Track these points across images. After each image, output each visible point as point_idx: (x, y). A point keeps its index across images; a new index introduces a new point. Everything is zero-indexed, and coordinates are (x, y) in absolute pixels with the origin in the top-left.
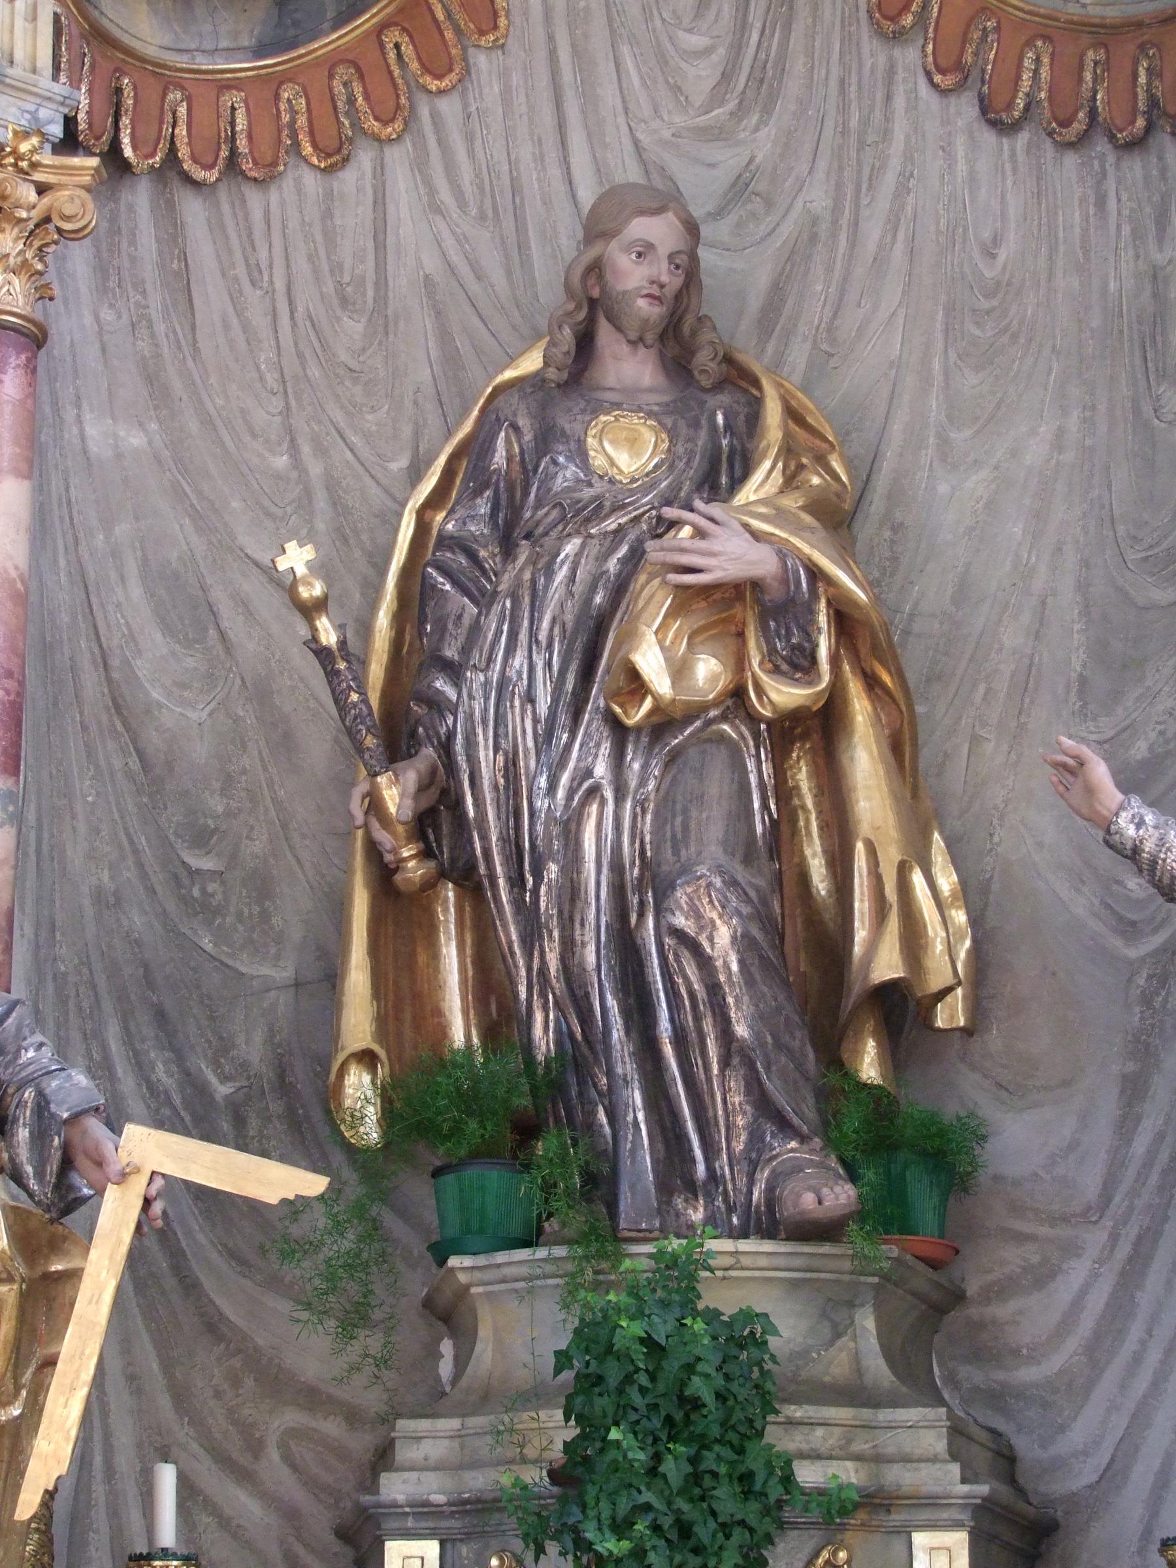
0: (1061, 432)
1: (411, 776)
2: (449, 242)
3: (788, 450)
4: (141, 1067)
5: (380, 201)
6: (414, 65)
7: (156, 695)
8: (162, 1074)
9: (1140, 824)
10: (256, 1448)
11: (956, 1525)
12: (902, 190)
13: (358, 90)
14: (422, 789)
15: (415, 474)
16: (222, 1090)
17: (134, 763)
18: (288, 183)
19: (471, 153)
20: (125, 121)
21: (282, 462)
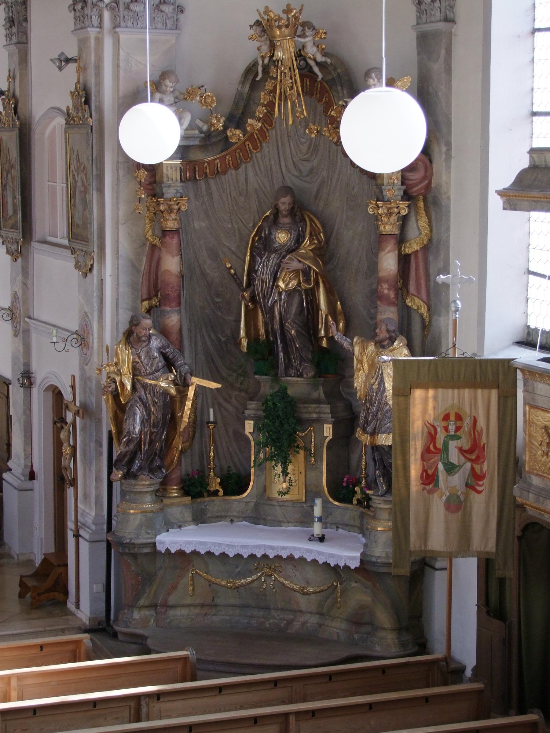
0: (364, 226)
1: (249, 293)
2: (259, 181)
3: (311, 235)
4: (209, 336)
5: (246, 175)
6: (251, 148)
7: (209, 272)
8: (213, 337)
9: (338, 338)
10: (231, 398)
11: (330, 424)
12: (339, 174)
13: (241, 154)
14: (251, 293)
15: (254, 227)
16: (223, 339)
17: (206, 283)
18: (229, 172)
19: (263, 163)
20: (197, 173)
21: (230, 226)
